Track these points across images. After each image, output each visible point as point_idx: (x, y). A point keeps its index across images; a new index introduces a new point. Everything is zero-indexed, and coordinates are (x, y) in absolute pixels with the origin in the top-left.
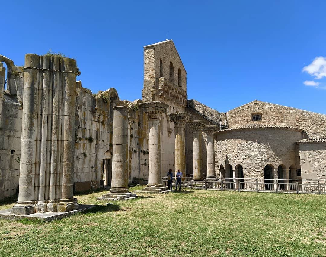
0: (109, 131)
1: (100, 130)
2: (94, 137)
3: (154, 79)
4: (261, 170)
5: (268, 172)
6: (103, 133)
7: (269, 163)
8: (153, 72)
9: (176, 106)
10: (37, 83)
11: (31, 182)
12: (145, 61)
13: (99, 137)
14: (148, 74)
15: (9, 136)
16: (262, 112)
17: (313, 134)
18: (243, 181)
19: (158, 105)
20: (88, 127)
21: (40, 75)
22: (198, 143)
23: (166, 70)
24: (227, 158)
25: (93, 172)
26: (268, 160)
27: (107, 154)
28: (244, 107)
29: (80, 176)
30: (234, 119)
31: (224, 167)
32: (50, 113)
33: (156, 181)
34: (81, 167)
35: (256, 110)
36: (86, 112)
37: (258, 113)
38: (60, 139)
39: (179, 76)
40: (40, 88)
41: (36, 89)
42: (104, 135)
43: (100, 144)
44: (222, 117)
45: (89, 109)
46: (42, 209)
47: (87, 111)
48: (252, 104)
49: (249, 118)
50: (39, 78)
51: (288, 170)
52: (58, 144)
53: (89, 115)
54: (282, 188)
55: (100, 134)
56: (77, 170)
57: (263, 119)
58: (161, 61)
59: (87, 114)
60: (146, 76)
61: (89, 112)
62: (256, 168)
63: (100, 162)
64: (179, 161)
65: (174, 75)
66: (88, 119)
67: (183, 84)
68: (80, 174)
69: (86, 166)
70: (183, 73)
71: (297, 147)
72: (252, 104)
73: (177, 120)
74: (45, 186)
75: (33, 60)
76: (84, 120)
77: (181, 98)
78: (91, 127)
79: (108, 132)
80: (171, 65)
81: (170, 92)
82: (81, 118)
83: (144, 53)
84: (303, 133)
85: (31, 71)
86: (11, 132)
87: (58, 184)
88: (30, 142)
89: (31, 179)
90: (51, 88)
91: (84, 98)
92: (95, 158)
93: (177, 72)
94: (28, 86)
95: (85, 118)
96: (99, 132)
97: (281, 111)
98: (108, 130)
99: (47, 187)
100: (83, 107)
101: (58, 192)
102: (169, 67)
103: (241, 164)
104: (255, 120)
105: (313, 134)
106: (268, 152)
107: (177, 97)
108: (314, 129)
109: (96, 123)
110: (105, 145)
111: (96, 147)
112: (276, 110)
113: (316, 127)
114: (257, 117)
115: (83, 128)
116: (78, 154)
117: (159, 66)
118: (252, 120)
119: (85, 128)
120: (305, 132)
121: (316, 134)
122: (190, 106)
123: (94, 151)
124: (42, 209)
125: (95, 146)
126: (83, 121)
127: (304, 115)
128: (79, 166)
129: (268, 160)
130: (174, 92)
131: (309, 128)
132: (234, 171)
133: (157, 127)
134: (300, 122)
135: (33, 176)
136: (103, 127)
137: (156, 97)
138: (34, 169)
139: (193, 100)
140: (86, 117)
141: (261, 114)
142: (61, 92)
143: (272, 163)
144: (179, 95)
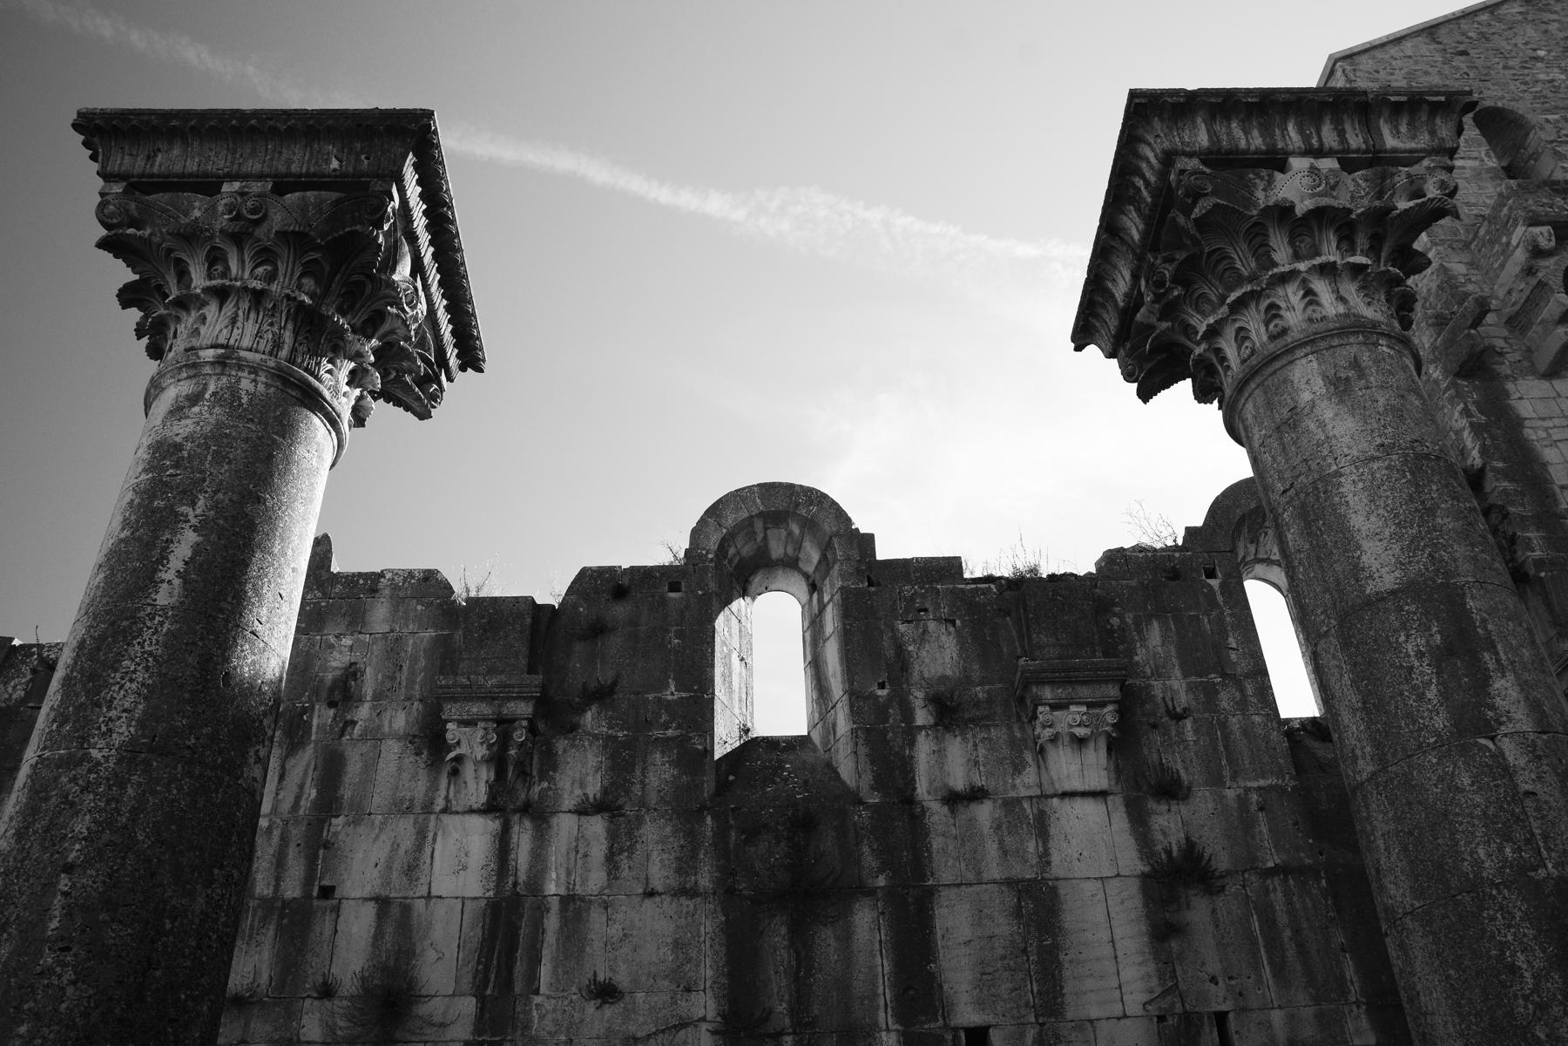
0: (705, 879)
1: (551, 888)
2: (443, 968)
6: (596, 918)
13: (535, 961)
42: (615, 931)
45: (399, 720)
47: (374, 736)
53: (391, 769)
55: (552, 922)
59: (370, 766)
66: (379, 799)
78: (411, 870)
82: (286, 806)
91: (347, 641)
96: (541, 909)
98: (686, 864)
100: (322, 717)
109: (492, 825)
115: (292, 889)
119: (327, 892)
126: (297, 833)
136: (598, 851)
140: (347, 793)
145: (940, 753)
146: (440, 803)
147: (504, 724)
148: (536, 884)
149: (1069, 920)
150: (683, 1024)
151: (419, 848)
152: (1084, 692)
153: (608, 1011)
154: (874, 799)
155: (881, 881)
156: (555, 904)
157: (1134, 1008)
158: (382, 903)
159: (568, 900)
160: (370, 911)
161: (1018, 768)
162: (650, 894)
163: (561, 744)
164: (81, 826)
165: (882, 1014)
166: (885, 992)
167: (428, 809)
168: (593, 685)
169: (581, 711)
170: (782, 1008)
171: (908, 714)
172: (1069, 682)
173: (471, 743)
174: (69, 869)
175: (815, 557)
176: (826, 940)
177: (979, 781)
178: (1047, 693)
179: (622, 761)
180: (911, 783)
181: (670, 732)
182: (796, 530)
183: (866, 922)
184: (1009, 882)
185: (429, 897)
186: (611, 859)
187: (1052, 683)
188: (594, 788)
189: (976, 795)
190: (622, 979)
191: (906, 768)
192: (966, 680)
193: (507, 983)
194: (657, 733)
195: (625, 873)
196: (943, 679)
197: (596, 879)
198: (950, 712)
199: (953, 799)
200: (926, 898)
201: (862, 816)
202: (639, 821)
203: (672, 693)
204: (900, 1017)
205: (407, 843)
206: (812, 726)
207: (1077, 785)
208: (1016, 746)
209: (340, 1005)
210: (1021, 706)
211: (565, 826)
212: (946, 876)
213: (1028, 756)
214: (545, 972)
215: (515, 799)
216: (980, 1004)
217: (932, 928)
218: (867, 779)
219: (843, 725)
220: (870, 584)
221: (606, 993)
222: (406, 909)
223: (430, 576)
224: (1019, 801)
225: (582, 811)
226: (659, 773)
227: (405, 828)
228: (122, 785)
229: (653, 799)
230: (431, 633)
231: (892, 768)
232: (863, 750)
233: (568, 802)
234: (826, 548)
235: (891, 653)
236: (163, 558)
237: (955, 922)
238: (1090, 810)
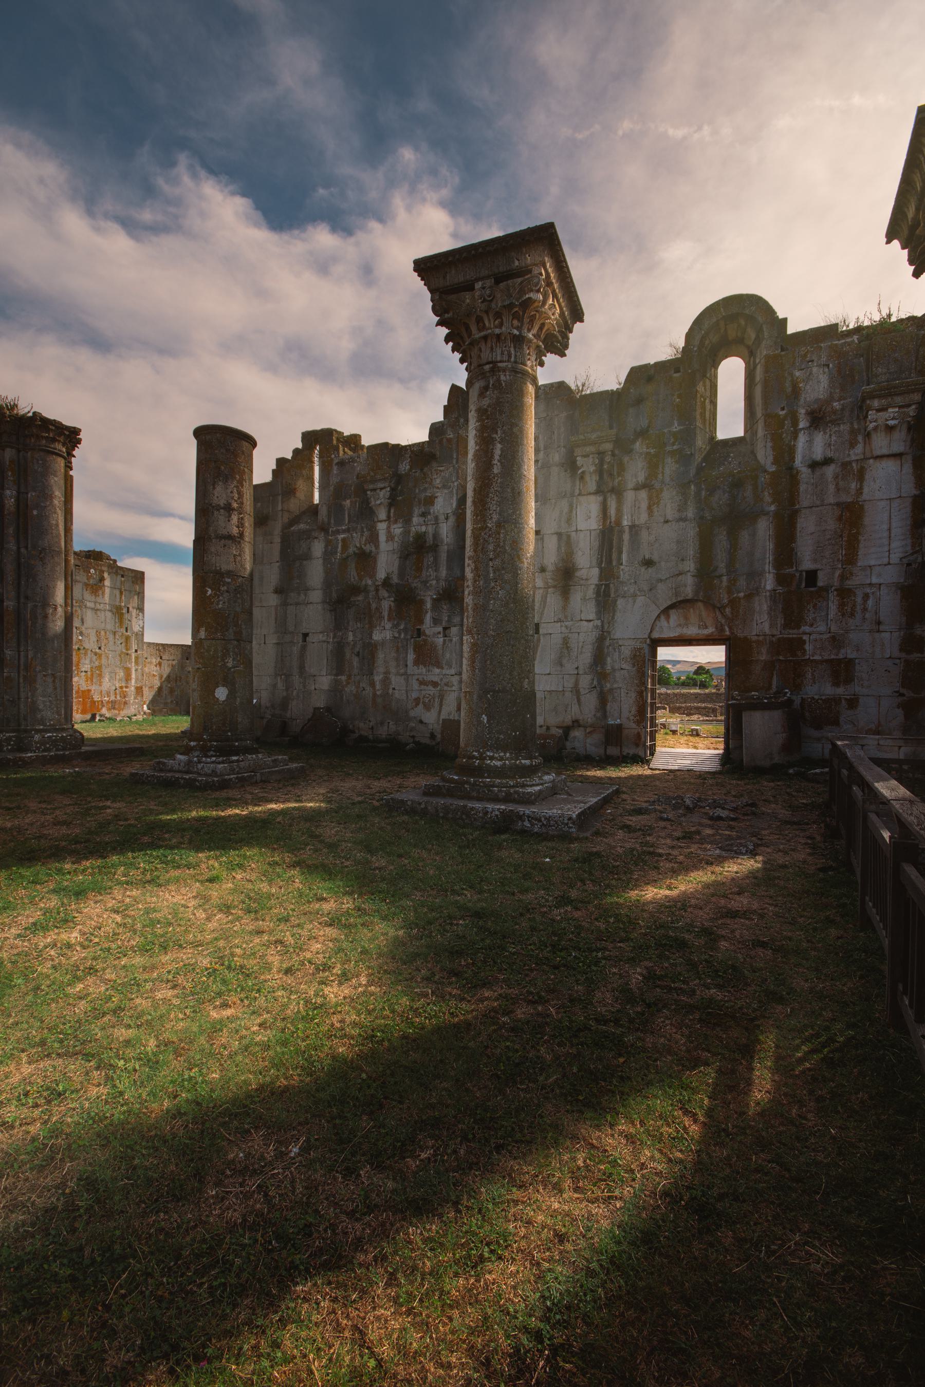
0: (690, 513)
6: (644, 535)
13: (620, 552)
15: (297, 604)
25: (582, 691)
27: (686, 618)
43: (624, 576)
55: (626, 537)
63: (627, 652)
78: (569, 521)
79: (681, 519)
86: (299, 594)
92: (592, 636)
96: (621, 532)
98: (682, 508)
109: (600, 498)
110: (661, 580)
111: (598, 593)
123: (590, 611)
125: (591, 593)
136: (644, 505)
145: (810, 442)
146: (577, 492)
147: (601, 454)
148: (618, 522)
149: (867, 521)
150: (681, 574)
151: (571, 511)
152: (899, 400)
153: (650, 570)
154: (773, 469)
155: (773, 508)
156: (627, 529)
157: (895, 558)
158: (559, 535)
159: (632, 527)
160: (555, 538)
161: (852, 445)
162: (667, 522)
163: (626, 459)
164: (491, 547)
165: (767, 566)
166: (769, 557)
167: (572, 495)
168: (638, 429)
169: (634, 442)
170: (722, 565)
171: (795, 422)
172: (890, 395)
173: (587, 465)
174: (491, 560)
175: (753, 336)
176: (744, 537)
177: (829, 454)
178: (876, 403)
179: (653, 464)
180: (792, 459)
181: (675, 447)
182: (742, 322)
184: (838, 504)
185: (577, 531)
186: (650, 508)
187: (879, 397)
188: (641, 478)
189: (827, 461)
190: (655, 557)
191: (792, 451)
192: (831, 399)
193: (610, 561)
194: (668, 448)
195: (656, 513)
196: (817, 400)
197: (643, 517)
198: (817, 419)
199: (814, 465)
200: (793, 516)
201: (763, 479)
202: (662, 490)
203: (676, 427)
204: (775, 567)
205: (566, 510)
206: (746, 431)
207: (885, 451)
208: (853, 432)
209: (548, 575)
210: (861, 409)
211: (629, 496)
212: (805, 503)
213: (860, 438)
214: (624, 557)
215: (608, 488)
216: (815, 561)
217: (795, 528)
218: (770, 459)
219: (760, 433)
220: (782, 350)
221: (648, 563)
222: (569, 537)
224: (850, 463)
225: (637, 488)
226: (670, 467)
227: (564, 504)
228: (499, 533)
229: (667, 479)
230: (564, 414)
231: (784, 455)
232: (769, 444)
233: (630, 485)
234: (759, 331)
235: (789, 390)
236: (492, 456)
237: (807, 525)
238: (890, 466)
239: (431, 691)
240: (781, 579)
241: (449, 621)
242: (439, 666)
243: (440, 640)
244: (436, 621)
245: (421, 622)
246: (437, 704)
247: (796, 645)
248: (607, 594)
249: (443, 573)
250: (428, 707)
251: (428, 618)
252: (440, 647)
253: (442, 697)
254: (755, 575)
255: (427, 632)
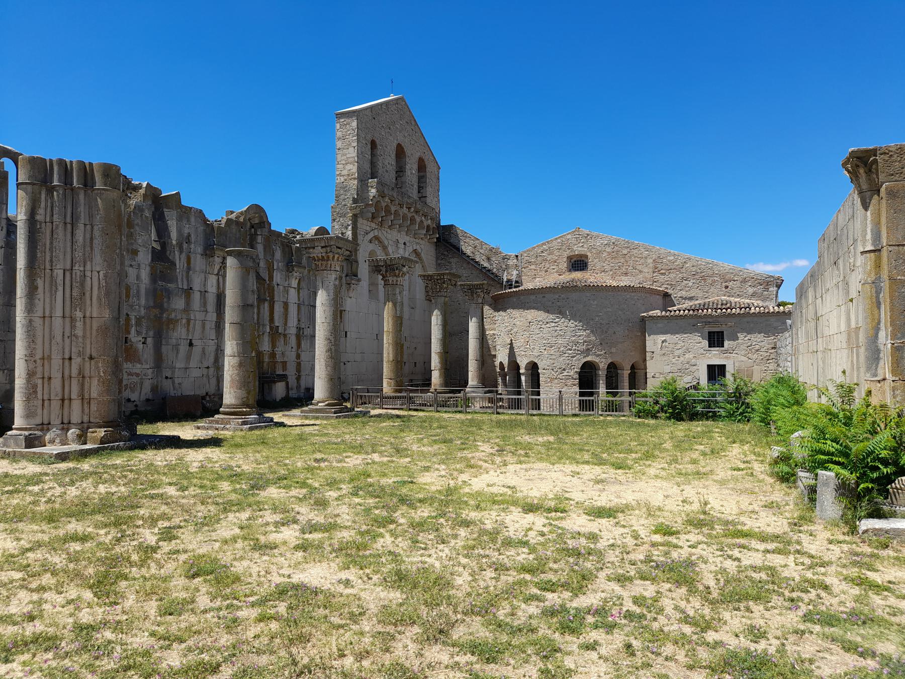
3: (356, 182)
4: (574, 372)
5: (587, 378)
7: (589, 359)
8: (354, 168)
9: (412, 239)
10: (41, 211)
11: (35, 392)
12: (339, 144)
14: (345, 172)
16: (588, 254)
17: (685, 299)
18: (538, 394)
19: (332, 243)
20: (197, 285)
21: (47, 195)
22: (440, 317)
23: (388, 161)
24: (512, 348)
26: (587, 352)
28: (555, 243)
29: (179, 384)
30: (533, 267)
31: (506, 365)
32: (68, 267)
33: (327, 395)
34: (183, 366)
35: (578, 250)
36: (192, 256)
37: (581, 256)
38: (88, 314)
39: (422, 174)
40: (48, 220)
41: (41, 223)
44: (510, 262)
45: (200, 250)
46: (57, 441)
48: (569, 237)
49: (564, 265)
50: (46, 201)
51: (626, 373)
52: (84, 322)
54: (612, 407)
56: (173, 372)
57: (590, 268)
58: (373, 144)
60: (340, 175)
61: (199, 256)
62: (564, 370)
64: (391, 356)
65: (408, 172)
66: (197, 269)
67: (429, 190)
68: (180, 380)
69: (193, 363)
70: (430, 168)
71: (643, 327)
72: (569, 237)
73: (386, 271)
74: (63, 400)
75: (33, 168)
76: (188, 273)
77: (422, 221)
80: (400, 152)
81: (393, 209)
83: (334, 127)
84: (666, 295)
85: (29, 187)
87: (86, 396)
88: (30, 321)
89: (35, 387)
90: (69, 220)
92: (215, 347)
93: (415, 167)
94: (24, 218)
95: (189, 268)
97: (625, 252)
99: (66, 402)
100: (185, 246)
101: (86, 411)
102: (393, 156)
103: (536, 361)
104: (576, 270)
105: (685, 299)
106: (588, 336)
107: (413, 220)
108: (687, 289)
112: (616, 248)
113: (691, 284)
114: (579, 264)
115: (185, 287)
116: (174, 341)
117: (369, 153)
118: (570, 271)
119: (191, 288)
120: (670, 295)
121: (691, 299)
122: (446, 240)
124: (57, 441)
126: (184, 274)
127: (669, 261)
128: (178, 365)
129: (587, 352)
130: (405, 210)
131: (679, 288)
132: (523, 374)
133: (331, 287)
134: (662, 274)
135: (40, 382)
137: (360, 220)
138: (40, 369)
139: (452, 226)
140: (192, 266)
141: (586, 256)
142: (89, 227)
143: (597, 360)
144: (416, 217)
183: (266, 305)
223: (201, 211)
231: (271, 278)
237: (278, 308)
239: (134, 379)
240: (271, 328)
241: (146, 334)
242: (140, 362)
243: (140, 346)
244: (138, 333)
245: (129, 333)
246: (139, 389)
247: (273, 355)
248: (219, 327)
249: (143, 302)
250: (133, 391)
251: (133, 330)
252: (141, 351)
253: (142, 384)
254: (264, 325)
255: (134, 340)
